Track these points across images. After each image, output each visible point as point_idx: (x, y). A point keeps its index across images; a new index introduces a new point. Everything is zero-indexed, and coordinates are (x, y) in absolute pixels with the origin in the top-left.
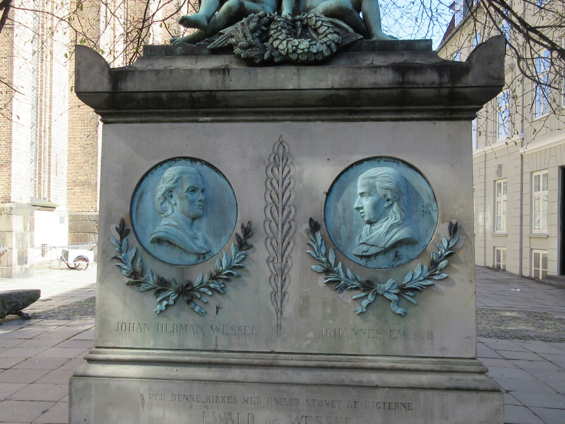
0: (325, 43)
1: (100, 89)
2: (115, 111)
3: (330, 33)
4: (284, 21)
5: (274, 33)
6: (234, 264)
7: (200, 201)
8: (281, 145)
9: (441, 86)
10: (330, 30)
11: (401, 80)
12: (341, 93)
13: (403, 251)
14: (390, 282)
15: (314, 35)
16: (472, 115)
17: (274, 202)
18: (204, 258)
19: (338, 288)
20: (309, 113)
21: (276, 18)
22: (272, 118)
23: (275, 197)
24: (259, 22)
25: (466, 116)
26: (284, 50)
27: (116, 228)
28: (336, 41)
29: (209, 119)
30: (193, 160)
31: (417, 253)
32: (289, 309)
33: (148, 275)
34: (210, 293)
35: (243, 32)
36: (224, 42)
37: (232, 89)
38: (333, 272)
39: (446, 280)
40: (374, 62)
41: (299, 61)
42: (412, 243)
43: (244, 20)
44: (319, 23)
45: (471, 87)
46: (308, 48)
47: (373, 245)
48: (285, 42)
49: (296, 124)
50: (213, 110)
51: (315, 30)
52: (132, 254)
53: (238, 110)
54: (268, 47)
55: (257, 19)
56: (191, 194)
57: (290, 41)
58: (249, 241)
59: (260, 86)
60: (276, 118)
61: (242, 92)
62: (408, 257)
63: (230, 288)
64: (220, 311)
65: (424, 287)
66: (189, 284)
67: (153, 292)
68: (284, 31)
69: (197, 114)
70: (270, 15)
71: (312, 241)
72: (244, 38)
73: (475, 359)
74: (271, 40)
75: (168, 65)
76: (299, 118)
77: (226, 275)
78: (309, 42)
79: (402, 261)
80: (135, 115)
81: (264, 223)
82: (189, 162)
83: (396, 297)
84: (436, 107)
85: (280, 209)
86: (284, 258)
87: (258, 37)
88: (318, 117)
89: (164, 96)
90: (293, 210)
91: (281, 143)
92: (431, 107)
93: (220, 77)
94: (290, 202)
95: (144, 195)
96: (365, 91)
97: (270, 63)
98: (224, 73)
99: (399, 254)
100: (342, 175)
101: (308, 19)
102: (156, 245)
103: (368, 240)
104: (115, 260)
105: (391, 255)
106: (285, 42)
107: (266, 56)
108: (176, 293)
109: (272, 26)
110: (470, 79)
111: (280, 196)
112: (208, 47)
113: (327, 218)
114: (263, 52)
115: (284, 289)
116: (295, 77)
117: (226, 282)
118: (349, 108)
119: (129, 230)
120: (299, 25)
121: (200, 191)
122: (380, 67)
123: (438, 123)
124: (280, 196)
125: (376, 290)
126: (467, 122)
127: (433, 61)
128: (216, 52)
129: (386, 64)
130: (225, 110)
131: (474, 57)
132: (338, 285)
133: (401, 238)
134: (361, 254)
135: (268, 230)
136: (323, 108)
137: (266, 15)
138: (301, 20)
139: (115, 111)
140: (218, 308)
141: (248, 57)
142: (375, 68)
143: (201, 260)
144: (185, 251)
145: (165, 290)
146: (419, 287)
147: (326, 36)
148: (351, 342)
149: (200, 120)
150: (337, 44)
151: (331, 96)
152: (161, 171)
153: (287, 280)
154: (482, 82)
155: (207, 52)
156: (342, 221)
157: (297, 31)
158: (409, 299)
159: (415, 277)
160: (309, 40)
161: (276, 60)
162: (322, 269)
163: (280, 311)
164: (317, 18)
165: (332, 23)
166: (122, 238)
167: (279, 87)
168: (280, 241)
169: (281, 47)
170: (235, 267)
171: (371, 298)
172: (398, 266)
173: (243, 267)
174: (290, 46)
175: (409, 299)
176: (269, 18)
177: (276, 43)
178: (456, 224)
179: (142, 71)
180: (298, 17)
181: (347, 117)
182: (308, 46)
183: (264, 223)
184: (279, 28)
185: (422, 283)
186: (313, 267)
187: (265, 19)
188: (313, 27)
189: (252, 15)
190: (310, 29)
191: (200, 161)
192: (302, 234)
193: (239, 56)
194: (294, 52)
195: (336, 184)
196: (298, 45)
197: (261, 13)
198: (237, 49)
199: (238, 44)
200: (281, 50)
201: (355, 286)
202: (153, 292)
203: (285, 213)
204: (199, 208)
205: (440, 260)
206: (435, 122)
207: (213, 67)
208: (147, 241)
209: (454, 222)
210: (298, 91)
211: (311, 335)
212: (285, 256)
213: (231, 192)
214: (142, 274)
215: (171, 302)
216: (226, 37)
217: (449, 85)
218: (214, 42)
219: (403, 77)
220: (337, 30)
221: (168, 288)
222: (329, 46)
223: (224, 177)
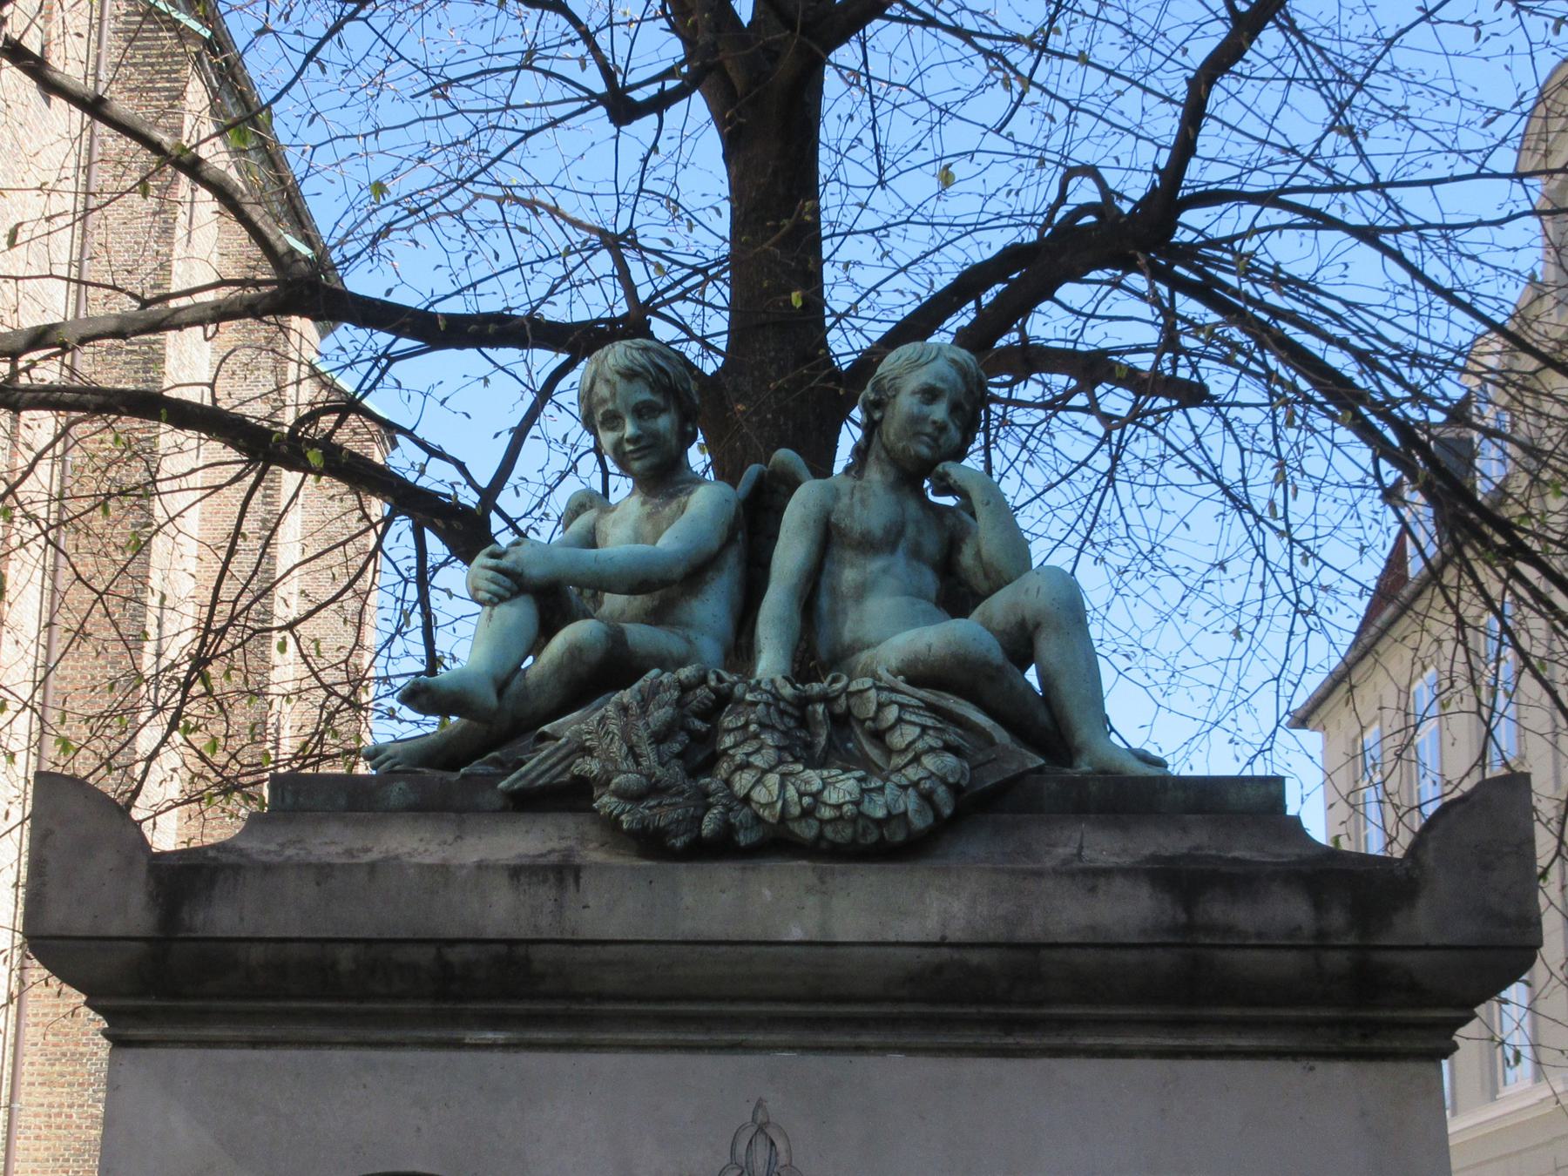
0: (915, 784)
1: (115, 928)
2: (157, 1003)
3: (931, 750)
4: (767, 705)
5: (736, 745)
9: (1322, 941)
10: (931, 740)
11: (1182, 918)
12: (975, 957)
15: (874, 753)
20: (861, 1023)
21: (739, 689)
22: (728, 1037)
24: (680, 703)
25: (1419, 1045)
26: (771, 805)
28: (951, 780)
29: (500, 1036)
35: (625, 738)
36: (559, 768)
37: (589, 937)
40: (1086, 852)
41: (824, 845)
43: (626, 696)
44: (892, 713)
45: (1427, 947)
46: (857, 803)
48: (773, 779)
49: (814, 1061)
50: (514, 1006)
53: (609, 1007)
54: (714, 793)
55: (676, 694)
57: (791, 774)
59: (687, 927)
60: (741, 1037)
61: (621, 948)
68: (768, 737)
69: (456, 1019)
70: (720, 679)
72: (630, 761)
74: (724, 768)
75: (358, 844)
76: (825, 1038)
78: (860, 780)
80: (231, 1017)
84: (1310, 1013)
87: (679, 756)
88: (892, 1039)
89: (345, 956)
91: (761, 1129)
92: (1292, 1013)
93: (545, 894)
96: (1058, 955)
97: (721, 848)
98: (561, 882)
101: (850, 695)
106: (773, 779)
107: (708, 826)
109: (728, 721)
112: (503, 784)
114: (699, 812)
116: (811, 901)
118: (1004, 1010)
120: (820, 717)
122: (1107, 872)
123: (1321, 1067)
126: (1424, 1068)
127: (1290, 852)
128: (528, 802)
129: (1126, 861)
130: (558, 1006)
131: (1431, 845)
136: (909, 1009)
137: (703, 680)
138: (827, 699)
139: (157, 1003)
141: (645, 829)
142: (1093, 876)
147: (916, 759)
149: (467, 1041)
150: (955, 789)
151: (939, 969)
154: (1466, 930)
157: (814, 735)
160: (858, 774)
161: (743, 839)
164: (884, 696)
165: (931, 708)
167: (756, 933)
169: (760, 795)
174: (791, 792)
176: (715, 691)
177: (742, 782)
179: (268, 868)
180: (816, 687)
181: (995, 1041)
182: (856, 795)
184: (753, 727)
187: (701, 692)
188: (869, 723)
189: (654, 672)
190: (858, 731)
193: (612, 823)
194: (807, 813)
196: (820, 792)
198: (605, 799)
199: (609, 781)
200: (762, 805)
206: (1311, 1063)
207: (520, 856)
210: (822, 950)
216: (564, 752)
217: (1351, 940)
218: (523, 769)
219: (1188, 910)
220: (953, 737)
222: (927, 797)
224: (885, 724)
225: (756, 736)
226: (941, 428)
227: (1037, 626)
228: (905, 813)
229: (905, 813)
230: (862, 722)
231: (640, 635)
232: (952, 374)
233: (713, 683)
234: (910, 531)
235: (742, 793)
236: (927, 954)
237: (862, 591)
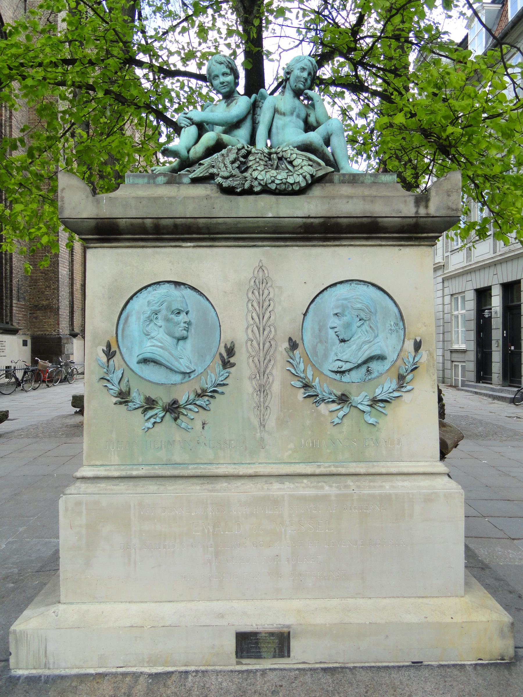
0: (302, 174)
3: (305, 165)
6: (218, 382)
7: (185, 322)
8: (261, 270)
13: (374, 366)
16: (433, 243)
17: (255, 323)
18: (190, 377)
19: (316, 402)
23: (255, 317)
24: (237, 153)
26: (263, 180)
27: (103, 350)
30: (177, 284)
31: (387, 367)
32: (271, 423)
33: (134, 394)
34: (196, 410)
38: (311, 387)
39: (412, 391)
41: (277, 191)
42: (382, 359)
43: (224, 151)
47: (347, 362)
48: (263, 172)
51: (291, 163)
52: (119, 374)
56: (177, 316)
58: (232, 360)
62: (378, 371)
63: (214, 404)
64: (206, 427)
65: (393, 399)
66: (175, 402)
67: (141, 410)
70: (248, 147)
71: (292, 358)
74: (250, 171)
77: (211, 392)
78: (287, 173)
79: (373, 376)
81: (247, 343)
82: (173, 286)
85: (261, 329)
86: (266, 375)
87: (237, 168)
90: (273, 330)
94: (269, 323)
95: (130, 318)
97: (250, 192)
99: (370, 369)
100: (318, 297)
102: (142, 366)
103: (343, 356)
104: (102, 380)
105: (363, 369)
107: (247, 186)
108: (164, 410)
109: (251, 158)
111: (261, 317)
113: (304, 338)
114: (244, 182)
115: (266, 404)
117: (211, 399)
119: (115, 351)
121: (185, 314)
124: (261, 317)
125: (350, 403)
132: (315, 399)
133: (372, 354)
134: (336, 370)
135: (250, 350)
137: (243, 147)
138: (277, 153)
143: (187, 379)
144: (171, 370)
145: (151, 408)
146: (389, 398)
147: (302, 167)
148: (328, 451)
150: (312, 176)
152: (146, 295)
153: (269, 396)
155: (189, 181)
156: (318, 340)
158: (380, 409)
159: (385, 390)
162: (301, 384)
163: (263, 425)
166: (108, 360)
168: (262, 360)
170: (219, 385)
171: (346, 410)
172: (370, 379)
173: (227, 384)
175: (380, 409)
176: (246, 150)
177: (255, 174)
178: (420, 341)
183: (247, 343)
184: (258, 160)
185: (391, 395)
186: (292, 383)
188: (288, 159)
191: (184, 284)
192: (282, 352)
193: (220, 186)
194: (273, 182)
195: (312, 305)
197: (239, 146)
199: (218, 175)
200: (261, 180)
201: (331, 400)
202: (141, 410)
203: (266, 333)
204: (185, 329)
205: (406, 374)
208: (133, 363)
210: (277, 219)
211: (291, 446)
212: (266, 373)
213: (214, 314)
214: (129, 393)
215: (158, 420)
220: (311, 163)
221: (155, 406)
222: (304, 177)
223: (208, 299)
224: (292, 159)
225: (258, 162)
226: (306, 80)
227: (331, 134)
228: (299, 182)
229: (299, 182)
230: (286, 159)
231: (226, 138)
232: (309, 64)
233: (246, 148)
234: (297, 110)
235: (255, 177)
236: (304, 220)
237: (284, 126)
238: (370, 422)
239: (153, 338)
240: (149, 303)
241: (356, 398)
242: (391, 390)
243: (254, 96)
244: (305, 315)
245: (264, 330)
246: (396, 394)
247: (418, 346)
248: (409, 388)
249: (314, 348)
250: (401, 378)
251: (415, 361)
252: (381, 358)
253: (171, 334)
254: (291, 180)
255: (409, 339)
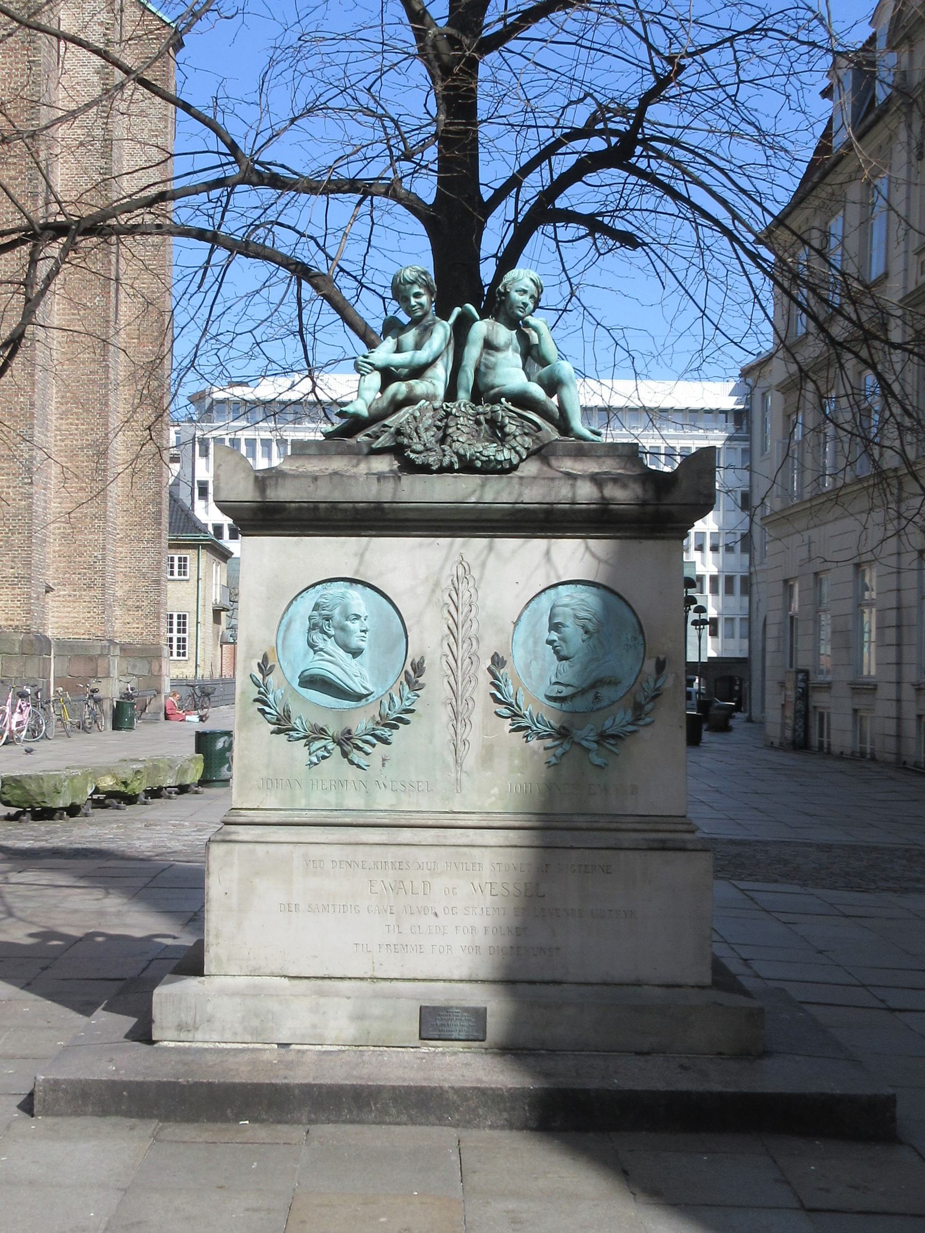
14: (590, 726)
32: (471, 759)
34: (375, 741)
63: (395, 736)
64: (387, 764)
66: (349, 732)
73: (684, 817)
74: (449, 440)
83: (595, 746)
90: (474, 643)
105: (590, 696)
110: (678, 496)
119: (274, 666)
126: (678, 542)
140: (384, 760)
159: (617, 721)
172: (598, 709)
177: (456, 445)
185: (624, 729)
195: (526, 612)
203: (465, 645)
209: (662, 657)
238: (596, 763)
239: (321, 650)
240: (317, 607)
241: (579, 732)
242: (624, 723)
243: (457, 310)
244: (516, 624)
245: (463, 642)
246: (631, 728)
247: (661, 666)
248: (648, 720)
249: (528, 666)
250: (638, 708)
251: (658, 685)
252: (613, 682)
253: (346, 648)
254: (500, 457)
255: (650, 658)
